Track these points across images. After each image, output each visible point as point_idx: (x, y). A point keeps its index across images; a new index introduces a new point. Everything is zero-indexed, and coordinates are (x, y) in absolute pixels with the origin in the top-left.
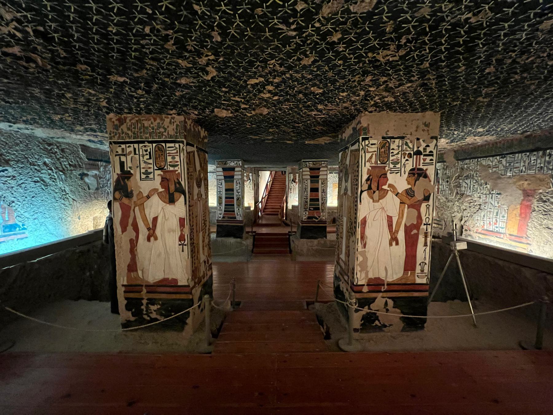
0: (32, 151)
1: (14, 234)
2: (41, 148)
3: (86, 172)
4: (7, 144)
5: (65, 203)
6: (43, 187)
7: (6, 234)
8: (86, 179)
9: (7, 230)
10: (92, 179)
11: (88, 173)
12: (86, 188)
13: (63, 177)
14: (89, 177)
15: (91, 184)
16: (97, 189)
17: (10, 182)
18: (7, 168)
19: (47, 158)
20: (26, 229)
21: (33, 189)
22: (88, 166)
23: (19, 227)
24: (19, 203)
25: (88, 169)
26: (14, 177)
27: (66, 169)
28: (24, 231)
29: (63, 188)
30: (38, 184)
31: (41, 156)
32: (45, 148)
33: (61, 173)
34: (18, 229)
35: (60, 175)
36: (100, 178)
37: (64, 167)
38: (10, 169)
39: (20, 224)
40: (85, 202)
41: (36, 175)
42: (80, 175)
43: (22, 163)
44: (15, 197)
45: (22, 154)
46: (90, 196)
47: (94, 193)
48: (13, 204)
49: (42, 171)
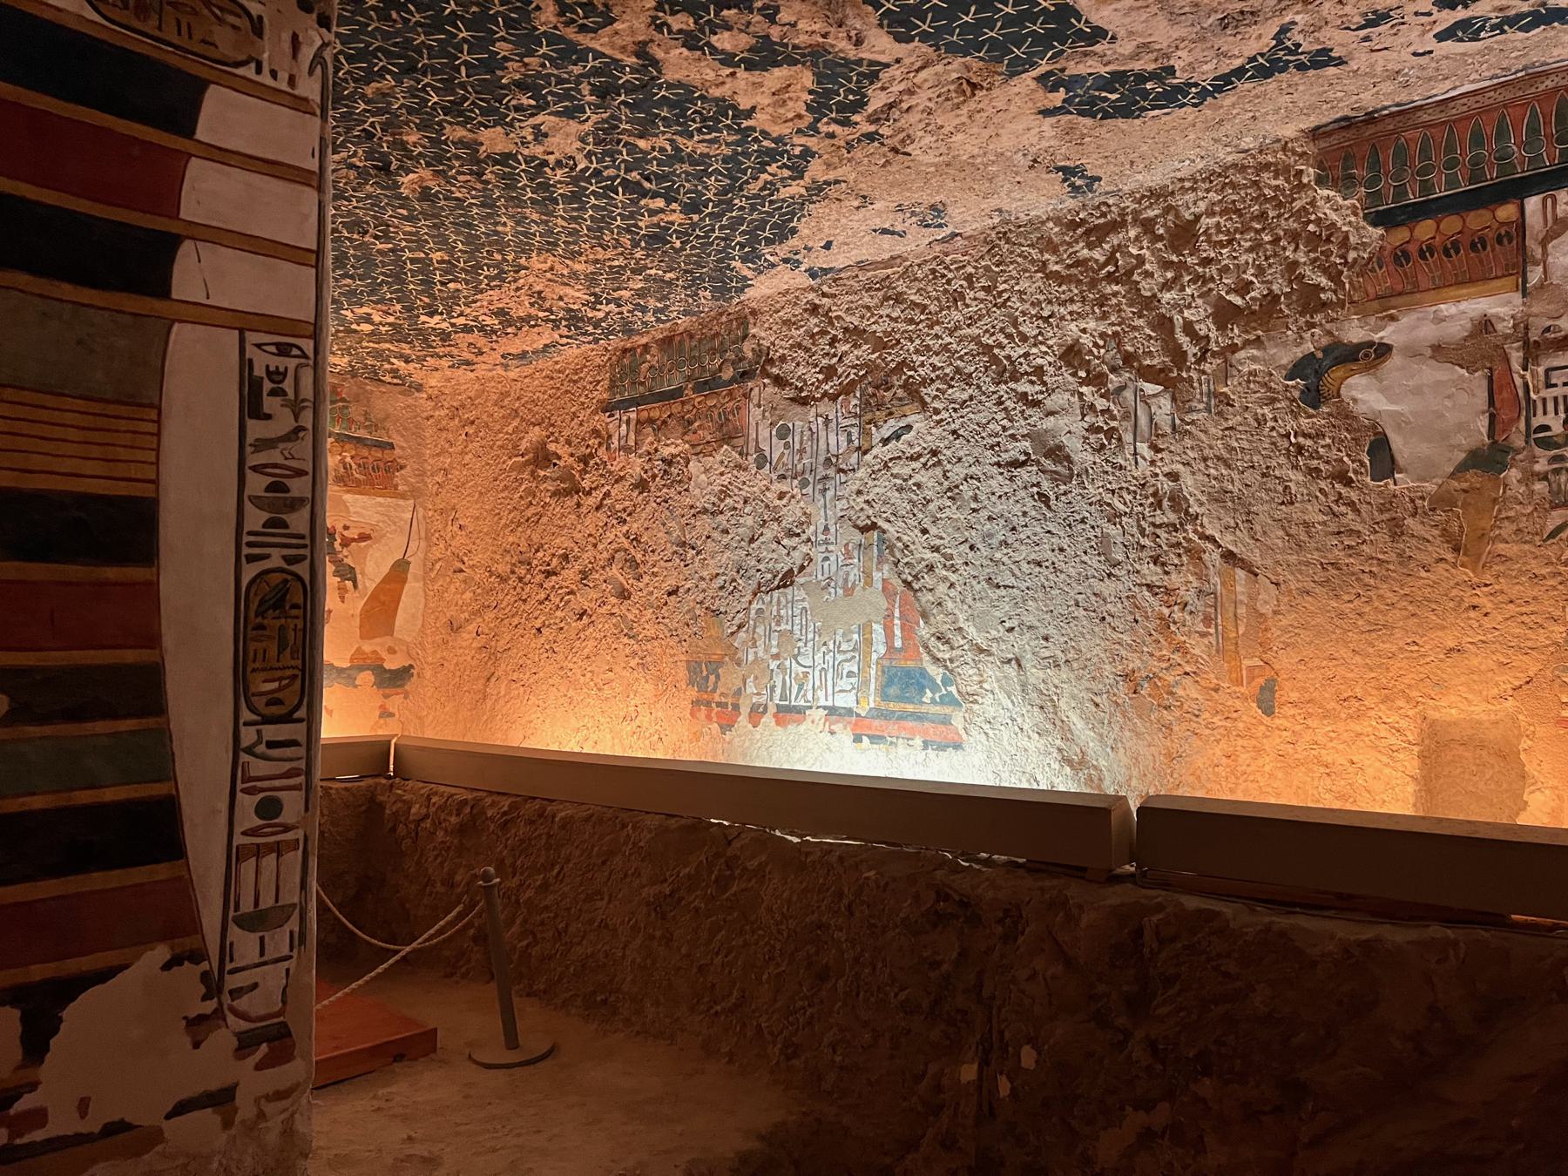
0: (1015, 302)
1: (920, 717)
2: (1050, 276)
3: (1355, 332)
5: (1175, 579)
6: (1046, 485)
8: (1363, 393)
9: (892, 691)
10: (1433, 373)
11: (1387, 334)
12: (1358, 462)
13: (1164, 407)
14: (1395, 360)
15: (1399, 420)
16: (1488, 459)
17: (917, 478)
18: (910, 420)
20: (954, 703)
21: (1000, 507)
22: (1385, 279)
24: (953, 577)
25: (1385, 304)
26: (934, 453)
27: (1192, 350)
28: (948, 710)
29: (1167, 486)
30: (1023, 474)
31: (1046, 320)
32: (1078, 263)
33: (1150, 388)
35: (1145, 399)
36: (1532, 351)
37: (1183, 340)
38: (917, 421)
40: (1333, 576)
42: (1296, 370)
43: (968, 379)
44: (936, 549)
45: (976, 339)
46: (1397, 530)
47: (1442, 501)
48: (928, 580)
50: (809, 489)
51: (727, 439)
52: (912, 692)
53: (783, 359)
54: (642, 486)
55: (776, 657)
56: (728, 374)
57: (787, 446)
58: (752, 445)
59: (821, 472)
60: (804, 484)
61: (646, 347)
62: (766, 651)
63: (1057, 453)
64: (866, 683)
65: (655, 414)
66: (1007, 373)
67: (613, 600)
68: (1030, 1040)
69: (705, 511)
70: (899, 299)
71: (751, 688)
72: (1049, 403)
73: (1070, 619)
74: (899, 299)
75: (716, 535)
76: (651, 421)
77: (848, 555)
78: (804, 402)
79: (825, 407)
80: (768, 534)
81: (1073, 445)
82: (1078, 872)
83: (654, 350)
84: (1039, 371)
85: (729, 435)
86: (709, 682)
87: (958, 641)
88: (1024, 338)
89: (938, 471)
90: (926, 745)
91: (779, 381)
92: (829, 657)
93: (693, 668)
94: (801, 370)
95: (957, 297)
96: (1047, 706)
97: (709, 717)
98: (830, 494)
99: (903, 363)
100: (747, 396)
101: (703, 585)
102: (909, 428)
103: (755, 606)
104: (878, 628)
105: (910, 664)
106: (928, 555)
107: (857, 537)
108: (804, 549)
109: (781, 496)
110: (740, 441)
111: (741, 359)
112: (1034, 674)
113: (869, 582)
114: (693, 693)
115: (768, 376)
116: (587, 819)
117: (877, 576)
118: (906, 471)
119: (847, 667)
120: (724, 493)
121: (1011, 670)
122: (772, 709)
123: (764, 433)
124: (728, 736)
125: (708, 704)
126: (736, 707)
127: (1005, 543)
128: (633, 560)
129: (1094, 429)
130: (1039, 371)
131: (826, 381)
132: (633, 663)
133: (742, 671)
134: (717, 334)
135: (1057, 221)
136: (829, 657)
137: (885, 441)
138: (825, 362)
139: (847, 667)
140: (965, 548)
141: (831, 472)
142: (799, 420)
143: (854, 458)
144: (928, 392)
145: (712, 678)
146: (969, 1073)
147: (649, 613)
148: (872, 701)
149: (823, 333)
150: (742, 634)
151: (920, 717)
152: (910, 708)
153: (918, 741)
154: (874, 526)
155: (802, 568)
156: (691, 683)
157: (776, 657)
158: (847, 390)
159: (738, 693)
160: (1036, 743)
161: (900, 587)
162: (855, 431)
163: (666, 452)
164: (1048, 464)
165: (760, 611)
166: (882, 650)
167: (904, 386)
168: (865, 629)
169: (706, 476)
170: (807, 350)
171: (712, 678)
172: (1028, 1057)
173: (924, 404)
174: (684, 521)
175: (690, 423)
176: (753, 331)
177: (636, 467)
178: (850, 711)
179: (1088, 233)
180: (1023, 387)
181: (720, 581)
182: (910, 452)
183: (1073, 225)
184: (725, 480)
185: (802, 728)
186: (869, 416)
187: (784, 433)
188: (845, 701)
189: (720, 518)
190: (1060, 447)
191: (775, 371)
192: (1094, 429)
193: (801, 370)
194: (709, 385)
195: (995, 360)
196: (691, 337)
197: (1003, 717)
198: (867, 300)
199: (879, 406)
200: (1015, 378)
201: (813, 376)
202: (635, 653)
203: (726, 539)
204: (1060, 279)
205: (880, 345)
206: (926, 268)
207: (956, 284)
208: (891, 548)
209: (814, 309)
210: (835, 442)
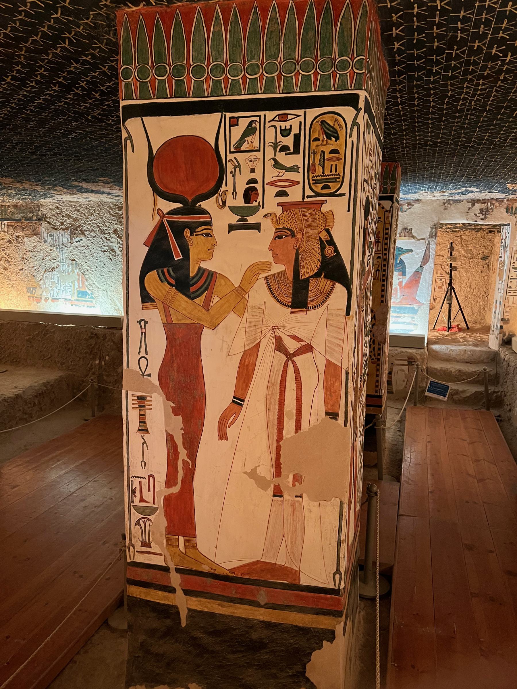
1: (86, 301)
2: (111, 214)
4: (84, 214)
6: (111, 257)
7: (80, 299)
9: (80, 295)
18: (82, 238)
19: (117, 224)
23: (89, 295)
26: (88, 246)
32: (117, 213)
34: (88, 296)
39: (89, 292)
41: (106, 244)
45: (96, 224)
48: (87, 273)
49: (112, 240)
50: (58, 250)
51: (35, 234)
52: (84, 296)
53: (50, 217)
54: (10, 242)
55: (51, 287)
56: (35, 218)
57: (52, 239)
58: (43, 238)
59: (61, 246)
60: (57, 248)
61: (9, 206)
62: (48, 285)
63: (113, 250)
64: (74, 294)
65: (13, 224)
66: (103, 232)
67: (2, 270)
68: (108, 355)
69: (30, 251)
70: (79, 211)
71: (45, 294)
72: (111, 240)
73: (116, 283)
74: (79, 211)
75: (33, 257)
76: (12, 226)
77: (68, 266)
78: (56, 229)
79: (61, 231)
80: (47, 258)
81: (116, 249)
82: (116, 328)
83: (11, 207)
84: (109, 233)
85: (36, 233)
86: (31, 290)
87: (94, 286)
88: (106, 226)
89: (89, 250)
90: (87, 306)
91: (49, 223)
92: (65, 288)
93: (28, 289)
94: (55, 221)
95: (92, 214)
96: (112, 299)
97: (33, 300)
98: (63, 252)
99: (80, 226)
100: (41, 225)
101: (30, 269)
102: (82, 240)
103: (45, 275)
104: (76, 283)
105: (84, 290)
106: (87, 267)
107: (71, 262)
108: (57, 263)
109: (51, 250)
110: (39, 236)
111: (38, 215)
112: (109, 293)
113: (74, 272)
114: (29, 294)
115: (46, 221)
116: (8, 323)
117: (75, 271)
118: (82, 249)
119: (69, 290)
120: (35, 247)
121: (105, 292)
122: (50, 298)
123: (46, 235)
124: (39, 304)
125: (33, 297)
126: (41, 298)
127: (103, 267)
128: (8, 260)
129: (120, 247)
130: (109, 233)
131: (62, 225)
132: (10, 286)
133: (42, 290)
134: (31, 208)
135: (112, 203)
136: (65, 288)
137: (77, 242)
138: (61, 221)
139: (69, 290)
140: (95, 267)
141: (64, 247)
142: (54, 233)
143: (69, 244)
144: (86, 233)
145: (34, 291)
146: (97, 362)
147: (14, 274)
148: (76, 297)
149: (60, 214)
150: (42, 281)
151: (86, 301)
152: (84, 299)
153: (86, 306)
154: (74, 260)
155: (57, 267)
156: (28, 292)
157: (51, 287)
158: (67, 229)
159: (41, 295)
160: (110, 306)
161: (81, 274)
162: (69, 239)
163: (17, 234)
164: (111, 252)
165: (46, 276)
166: (77, 287)
167: (81, 230)
168: (73, 282)
169: (29, 242)
170: (56, 217)
171: (34, 291)
172: (107, 358)
173: (85, 235)
174: (23, 252)
175: (24, 228)
176: (41, 209)
177: (8, 237)
178: (70, 300)
179: (118, 208)
180: (106, 236)
181: (35, 268)
182: (82, 245)
183: (115, 205)
184: (35, 244)
185: (58, 303)
186: (72, 236)
187: (51, 236)
188: (69, 297)
189: (34, 253)
190: (114, 249)
191: (48, 220)
192: (120, 247)
193: (55, 221)
194: (29, 220)
195: (100, 229)
196: (23, 206)
197: (103, 301)
198: (71, 209)
199: (75, 234)
200: (105, 233)
201: (58, 224)
202: (10, 284)
203: (36, 258)
204: (113, 216)
205: (74, 220)
206: (85, 206)
207: (92, 211)
208: (78, 265)
209: (58, 208)
210: (65, 240)
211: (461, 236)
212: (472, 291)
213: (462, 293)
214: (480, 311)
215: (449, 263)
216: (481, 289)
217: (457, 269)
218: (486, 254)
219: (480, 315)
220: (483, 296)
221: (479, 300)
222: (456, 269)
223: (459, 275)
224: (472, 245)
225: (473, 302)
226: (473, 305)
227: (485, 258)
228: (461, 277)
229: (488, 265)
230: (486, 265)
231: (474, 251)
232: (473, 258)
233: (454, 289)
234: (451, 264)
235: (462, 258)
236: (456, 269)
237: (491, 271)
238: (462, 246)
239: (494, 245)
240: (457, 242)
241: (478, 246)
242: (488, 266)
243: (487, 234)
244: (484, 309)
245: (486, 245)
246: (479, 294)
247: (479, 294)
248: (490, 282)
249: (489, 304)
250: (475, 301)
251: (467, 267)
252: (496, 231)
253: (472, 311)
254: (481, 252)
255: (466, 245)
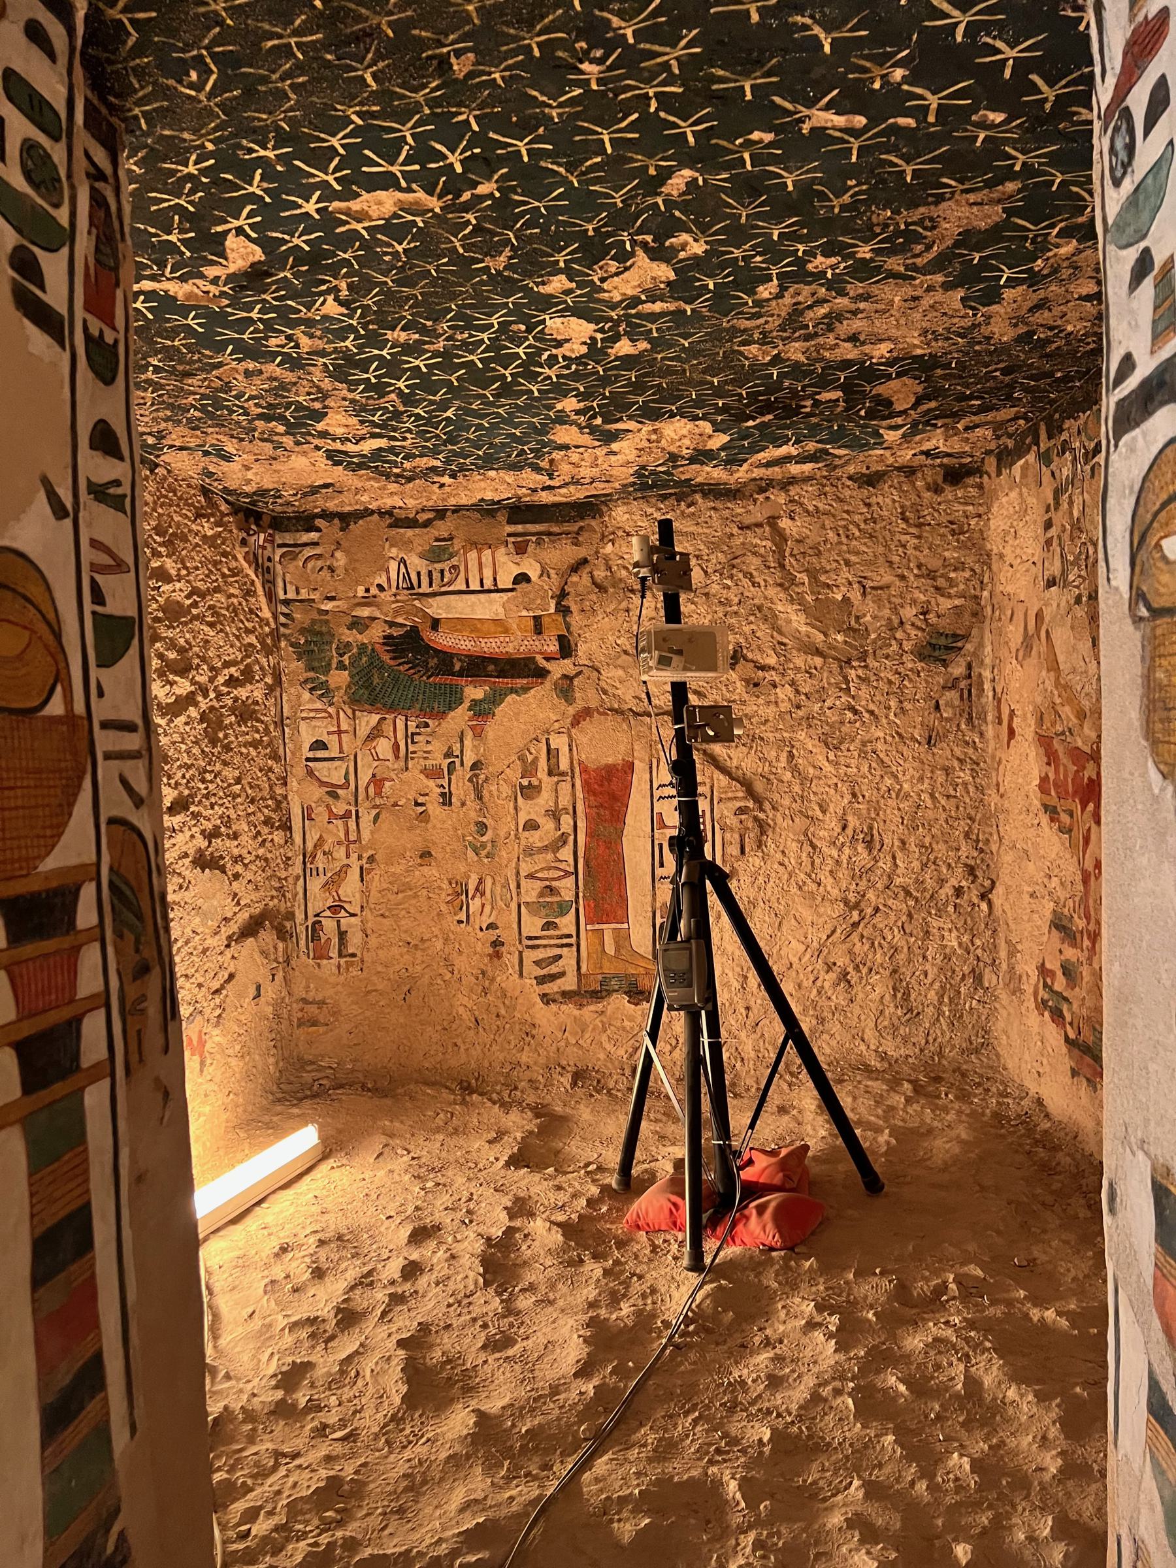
211: (772, 521)
212: (885, 864)
213: (828, 881)
214: (949, 992)
215: (661, 680)
216: (940, 849)
217: (731, 722)
218: (944, 624)
219: (957, 1016)
220: (959, 891)
221: (935, 923)
222: (721, 722)
223: (795, 770)
224: (846, 574)
225: (898, 938)
226: (901, 957)
227: (940, 647)
228: (804, 779)
229: (968, 688)
230: (952, 695)
231: (870, 612)
232: (863, 657)
233: (721, 881)
234: (679, 691)
235: (799, 661)
236: (721, 722)
237: (990, 731)
238: (787, 583)
239: (986, 558)
240: (754, 563)
241: (888, 578)
242: (967, 696)
243: (937, 490)
244: (978, 979)
245: (934, 563)
246: (930, 883)
247: (930, 883)
248: (992, 798)
249: (1003, 954)
250: (915, 927)
251: (833, 717)
252: (991, 464)
253: (902, 993)
254: (909, 613)
255: (813, 574)
